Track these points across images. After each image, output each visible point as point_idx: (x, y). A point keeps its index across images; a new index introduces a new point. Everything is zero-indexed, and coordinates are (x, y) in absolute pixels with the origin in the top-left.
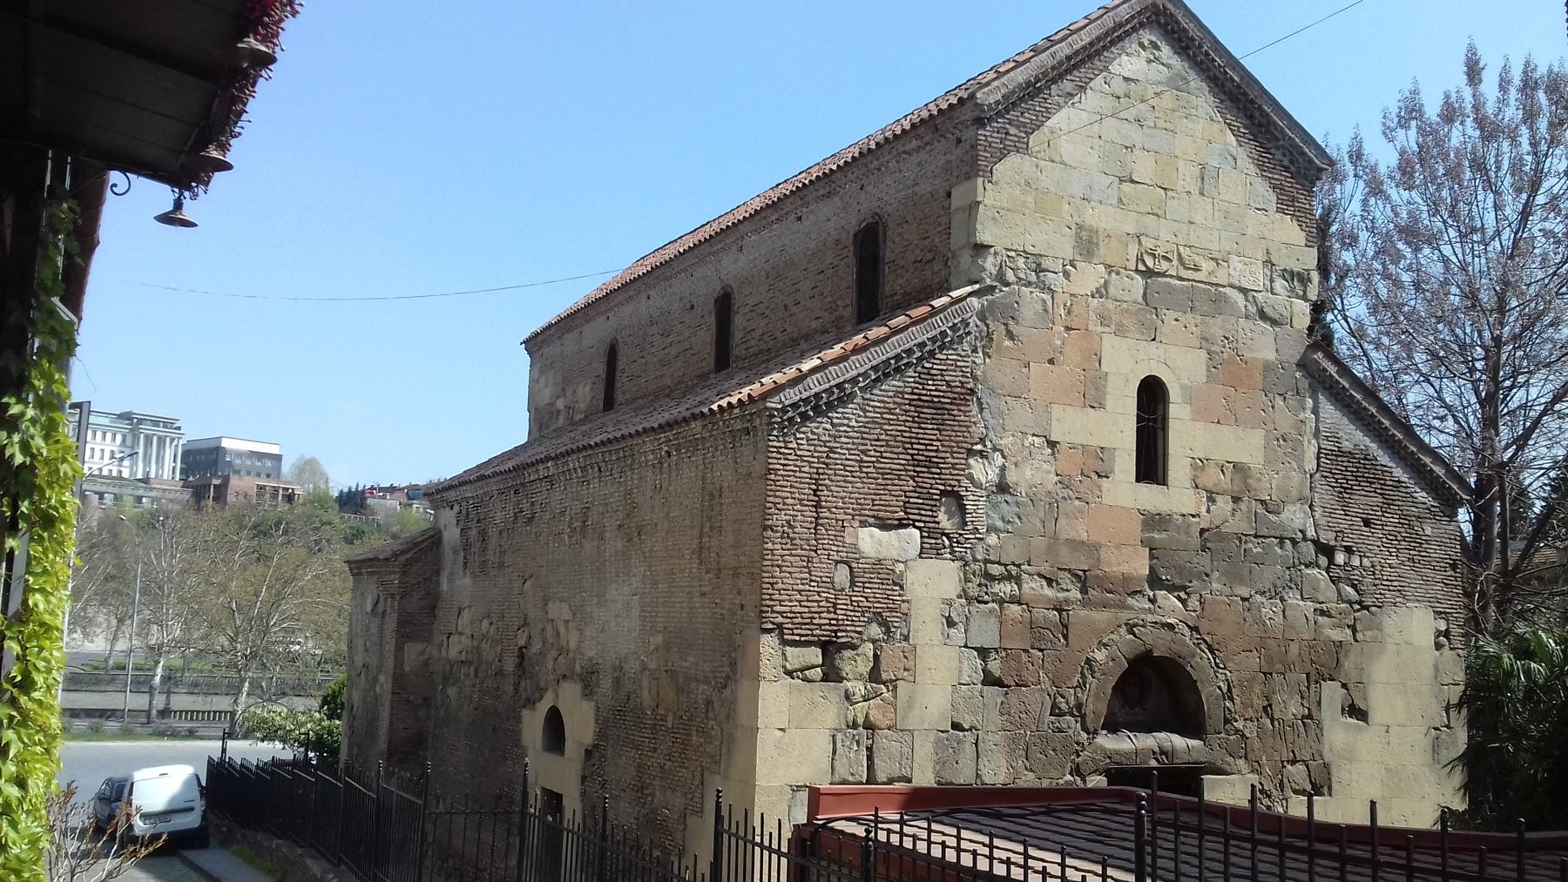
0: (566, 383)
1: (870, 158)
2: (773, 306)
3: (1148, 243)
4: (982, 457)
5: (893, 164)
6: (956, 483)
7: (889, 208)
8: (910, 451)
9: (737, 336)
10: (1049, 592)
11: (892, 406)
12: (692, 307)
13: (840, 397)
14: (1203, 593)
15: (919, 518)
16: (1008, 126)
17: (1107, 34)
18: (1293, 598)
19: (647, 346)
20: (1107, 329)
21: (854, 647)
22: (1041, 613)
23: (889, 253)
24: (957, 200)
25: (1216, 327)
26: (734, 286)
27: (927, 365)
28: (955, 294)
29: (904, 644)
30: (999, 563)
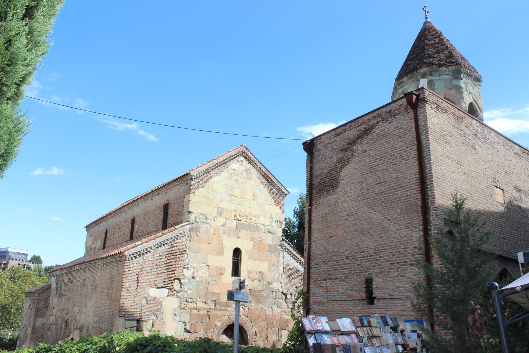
0: (95, 240)
1: (168, 185)
2: (144, 223)
3: (237, 212)
4: (187, 269)
5: (173, 188)
6: (179, 276)
7: (171, 200)
8: (166, 267)
9: (135, 231)
10: (205, 306)
11: (162, 255)
12: (126, 221)
13: (147, 251)
14: (249, 307)
16: (200, 181)
17: (228, 158)
18: (275, 307)
19: (115, 231)
21: (146, 322)
22: (202, 312)
23: (170, 211)
24: (186, 200)
25: (256, 235)
26: (136, 216)
27: (172, 244)
28: (182, 225)
29: (161, 321)
30: (191, 298)
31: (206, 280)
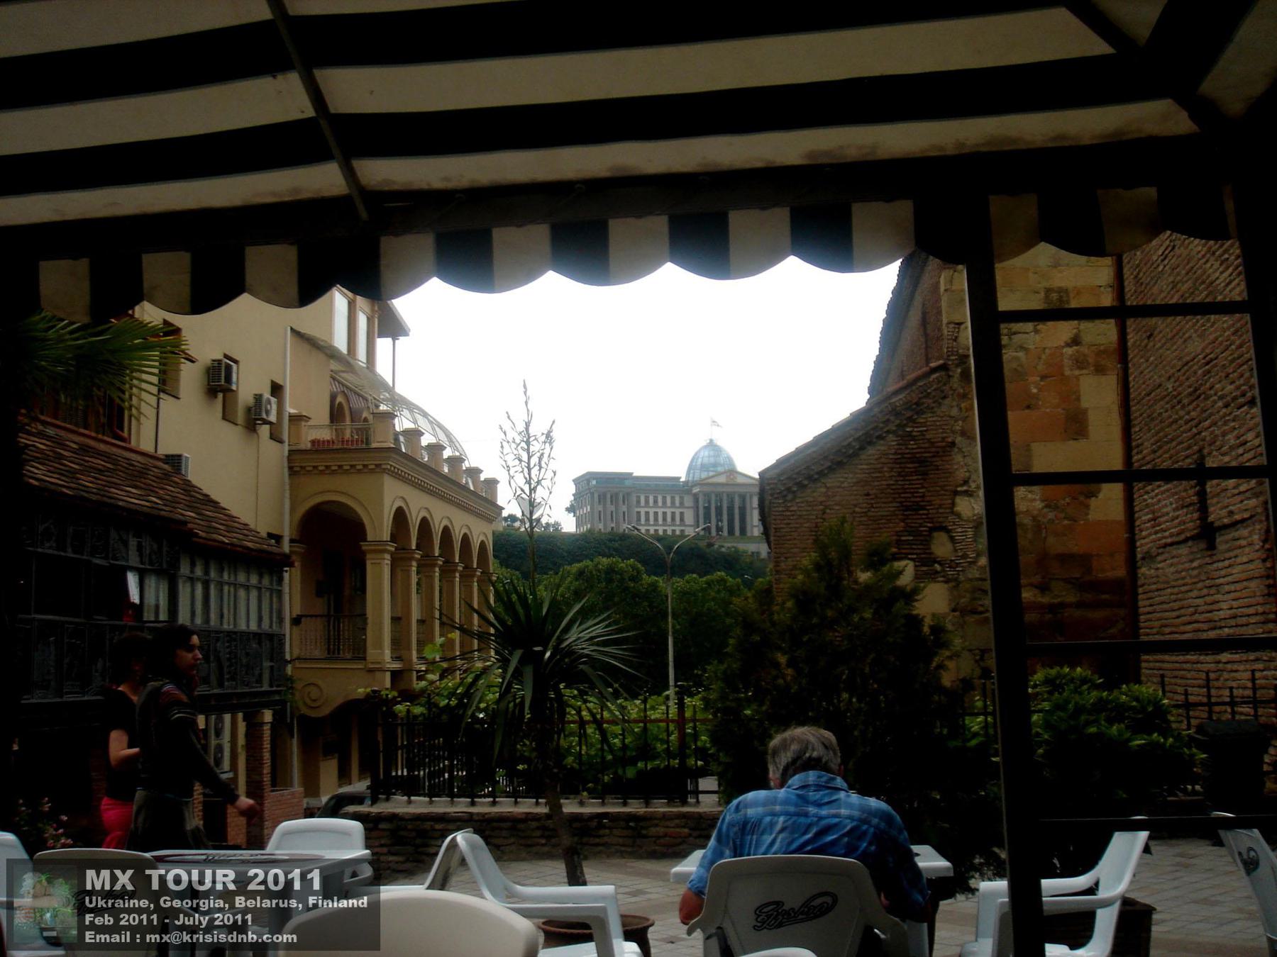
8: (898, 500)
15: (912, 551)
20: (1084, 371)
31: (1034, 518)
